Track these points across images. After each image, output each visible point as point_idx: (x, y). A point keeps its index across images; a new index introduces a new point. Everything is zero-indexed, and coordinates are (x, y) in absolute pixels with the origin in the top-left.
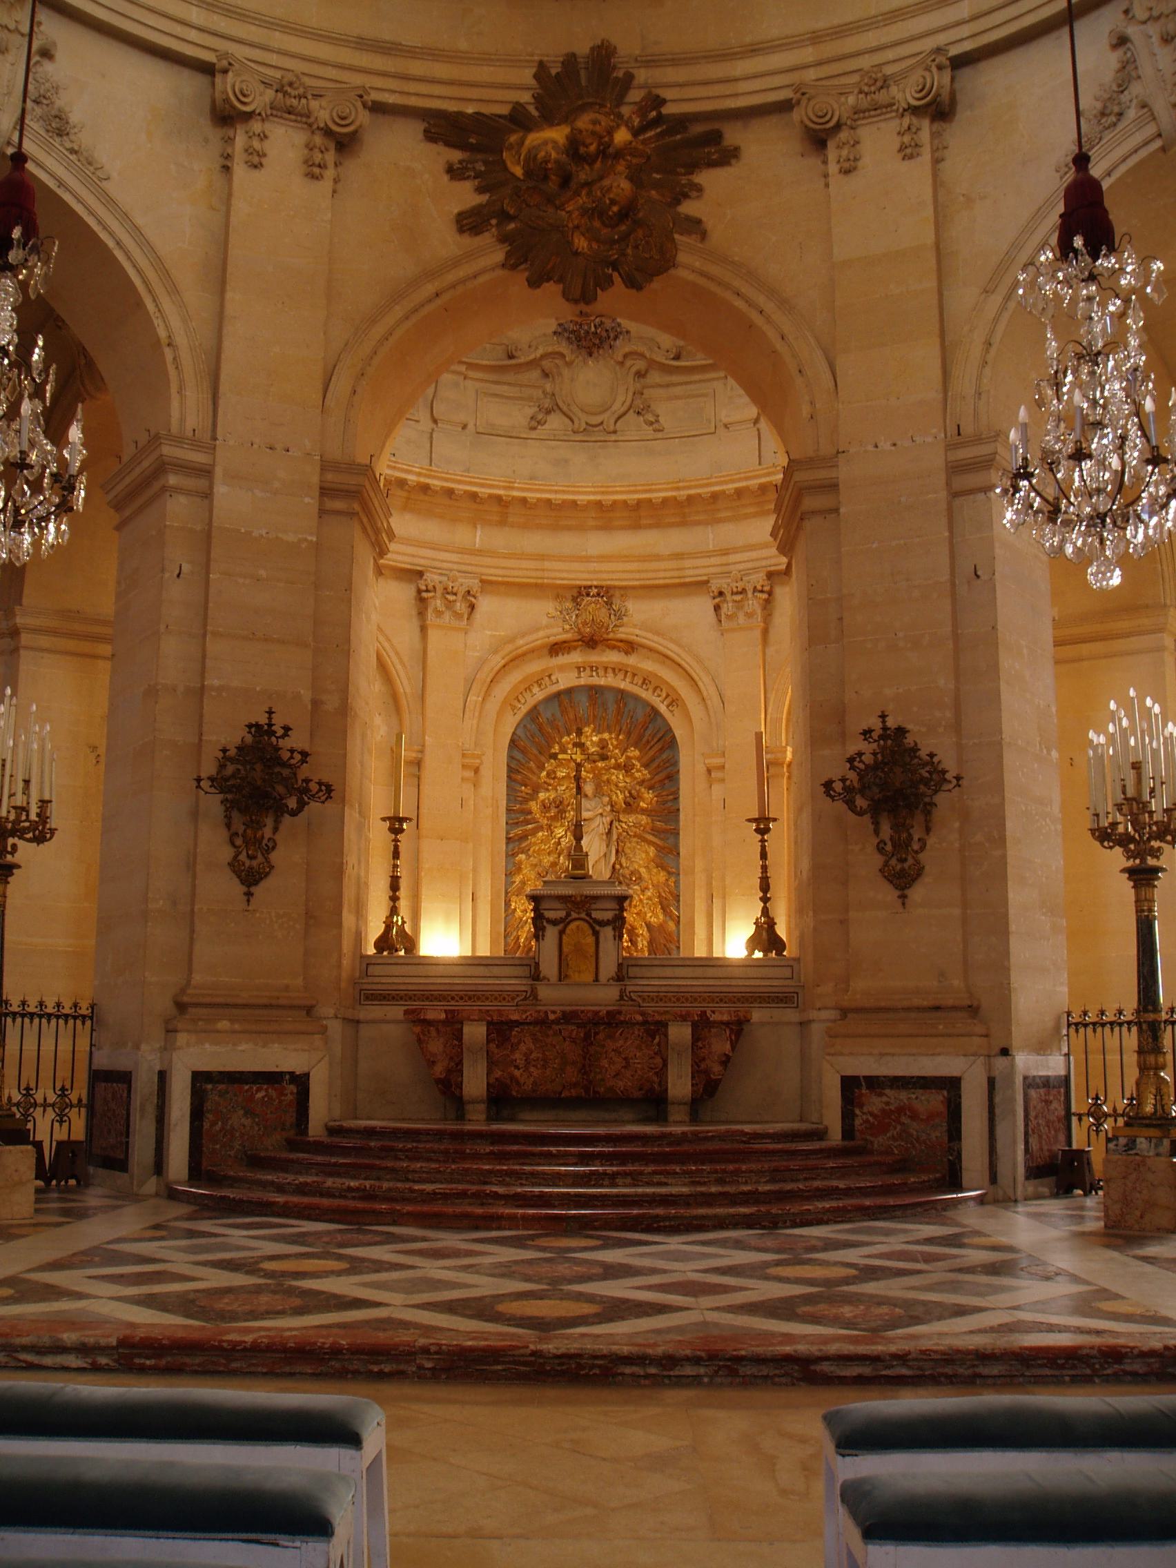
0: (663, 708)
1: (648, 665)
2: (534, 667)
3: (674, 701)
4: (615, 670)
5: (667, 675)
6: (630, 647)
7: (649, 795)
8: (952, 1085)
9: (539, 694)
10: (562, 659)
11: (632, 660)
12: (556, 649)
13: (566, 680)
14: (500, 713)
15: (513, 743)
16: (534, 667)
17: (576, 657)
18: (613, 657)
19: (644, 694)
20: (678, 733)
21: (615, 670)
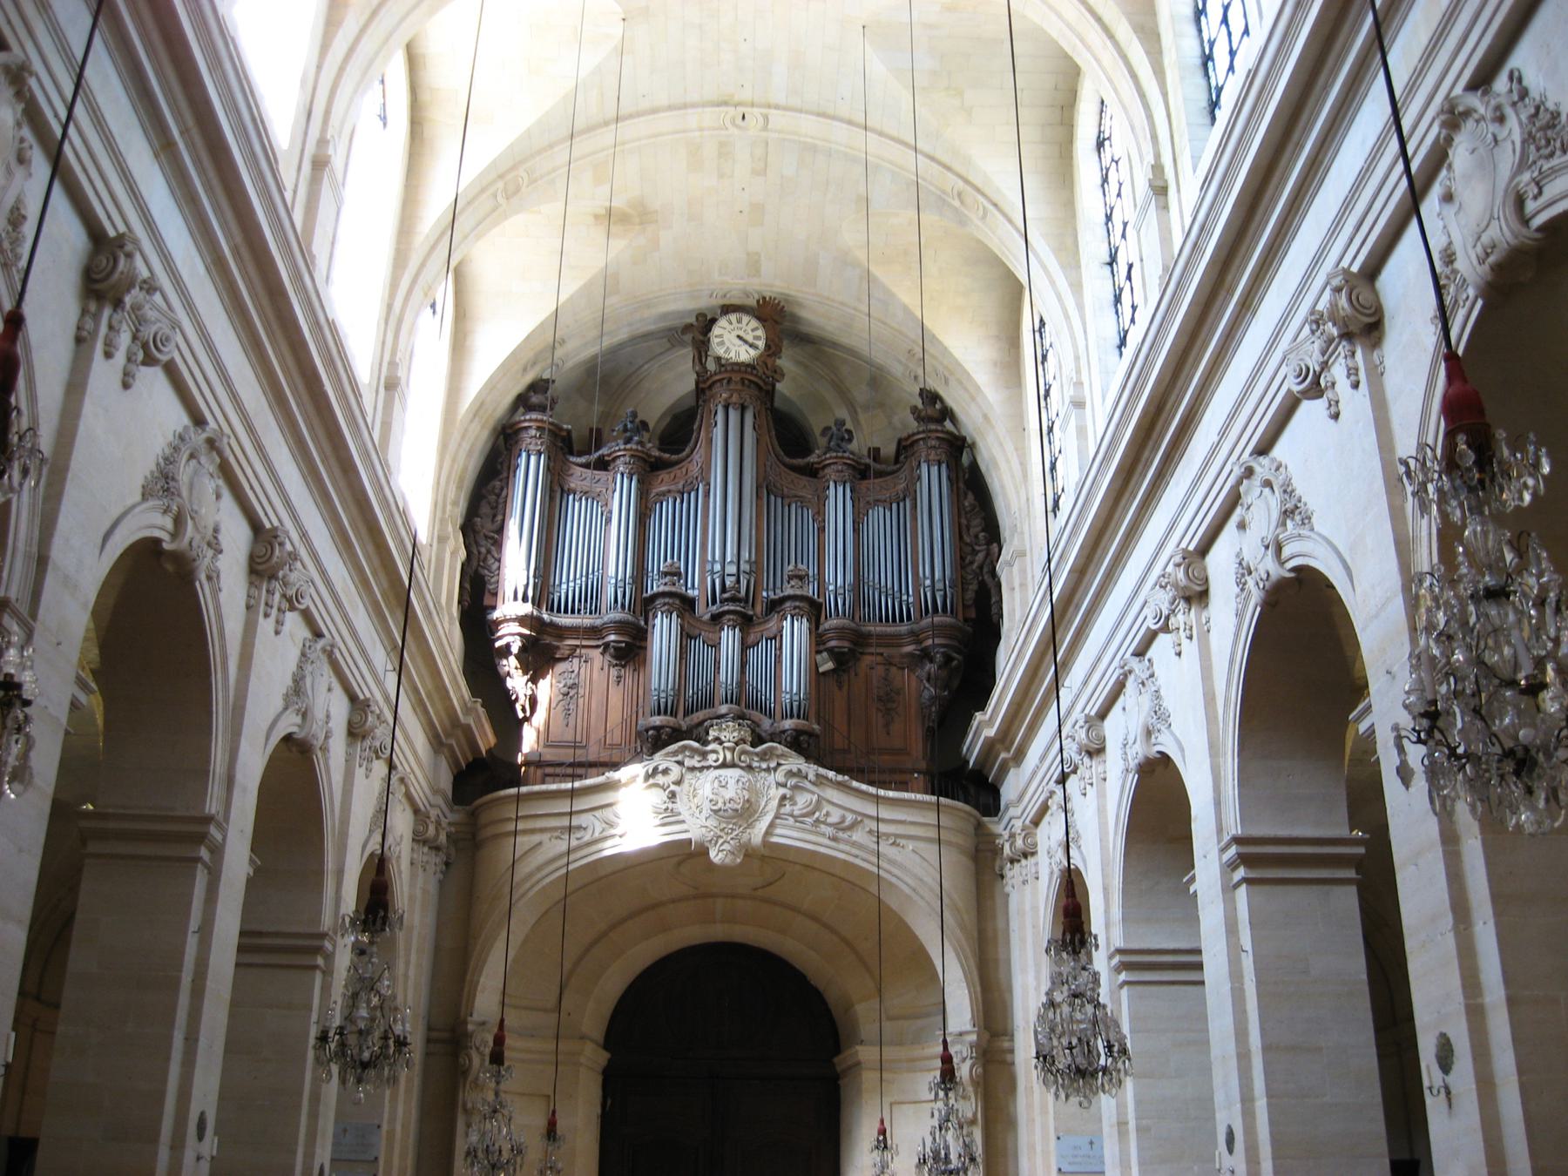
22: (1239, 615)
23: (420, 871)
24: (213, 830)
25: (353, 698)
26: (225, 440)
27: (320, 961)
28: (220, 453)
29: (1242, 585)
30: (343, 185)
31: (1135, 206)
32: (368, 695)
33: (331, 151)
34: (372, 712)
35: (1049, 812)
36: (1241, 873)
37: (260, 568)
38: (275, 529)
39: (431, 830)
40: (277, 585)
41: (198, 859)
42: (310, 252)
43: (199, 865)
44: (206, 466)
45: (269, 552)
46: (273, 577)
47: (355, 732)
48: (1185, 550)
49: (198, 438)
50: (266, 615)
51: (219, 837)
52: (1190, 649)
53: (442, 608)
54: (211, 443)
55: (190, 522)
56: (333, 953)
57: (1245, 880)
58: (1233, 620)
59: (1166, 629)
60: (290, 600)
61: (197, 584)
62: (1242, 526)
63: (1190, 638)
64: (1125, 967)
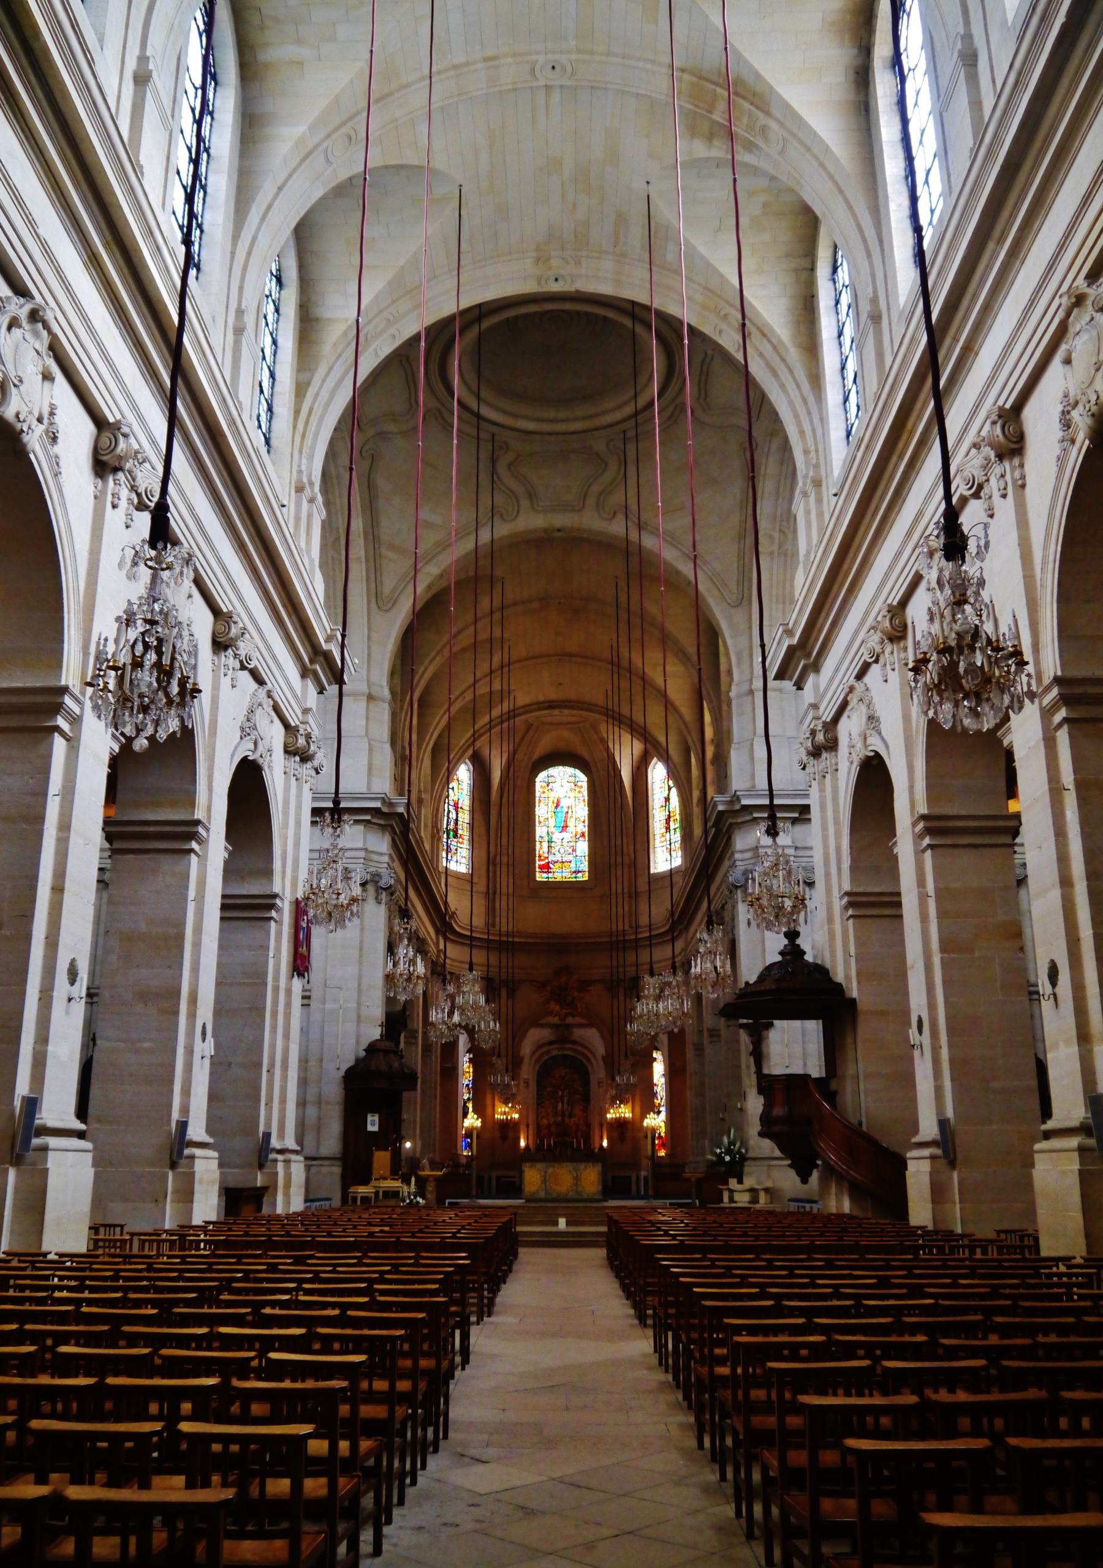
0: (584, 1061)
1: (580, 1048)
2: (544, 1049)
3: (589, 1060)
4: (570, 1049)
5: (586, 1052)
6: (574, 1042)
7: (581, 1089)
8: (629, 1178)
9: (546, 1057)
10: (554, 1046)
11: (575, 1047)
12: (551, 1043)
13: (555, 1053)
14: (534, 1066)
15: (538, 1073)
16: (544, 1049)
17: (557, 1046)
18: (569, 1046)
19: (579, 1057)
20: (590, 1069)
21: (570, 1049)
22: (1061, 460)
23: (293, 779)
24: (68, 700)
25: (216, 611)
26: (48, 312)
27: (194, 845)
28: (46, 326)
29: (1066, 424)
30: (173, 116)
31: (939, 96)
32: (231, 608)
33: (151, 66)
34: (235, 623)
35: (849, 708)
36: (1062, 714)
37: (104, 458)
38: (119, 422)
39: (301, 741)
40: (120, 476)
41: (57, 729)
42: (138, 161)
43: (56, 734)
44: (32, 342)
45: (113, 444)
46: (116, 470)
47: (220, 645)
48: (1001, 409)
49: (20, 308)
50: (114, 506)
51: (76, 709)
52: (1005, 509)
53: (302, 550)
54: (35, 316)
55: (14, 391)
56: (207, 840)
57: (1065, 720)
58: (1054, 469)
59: (976, 495)
60: (139, 495)
61: (32, 456)
62: (1068, 361)
63: (1004, 496)
64: (929, 831)
